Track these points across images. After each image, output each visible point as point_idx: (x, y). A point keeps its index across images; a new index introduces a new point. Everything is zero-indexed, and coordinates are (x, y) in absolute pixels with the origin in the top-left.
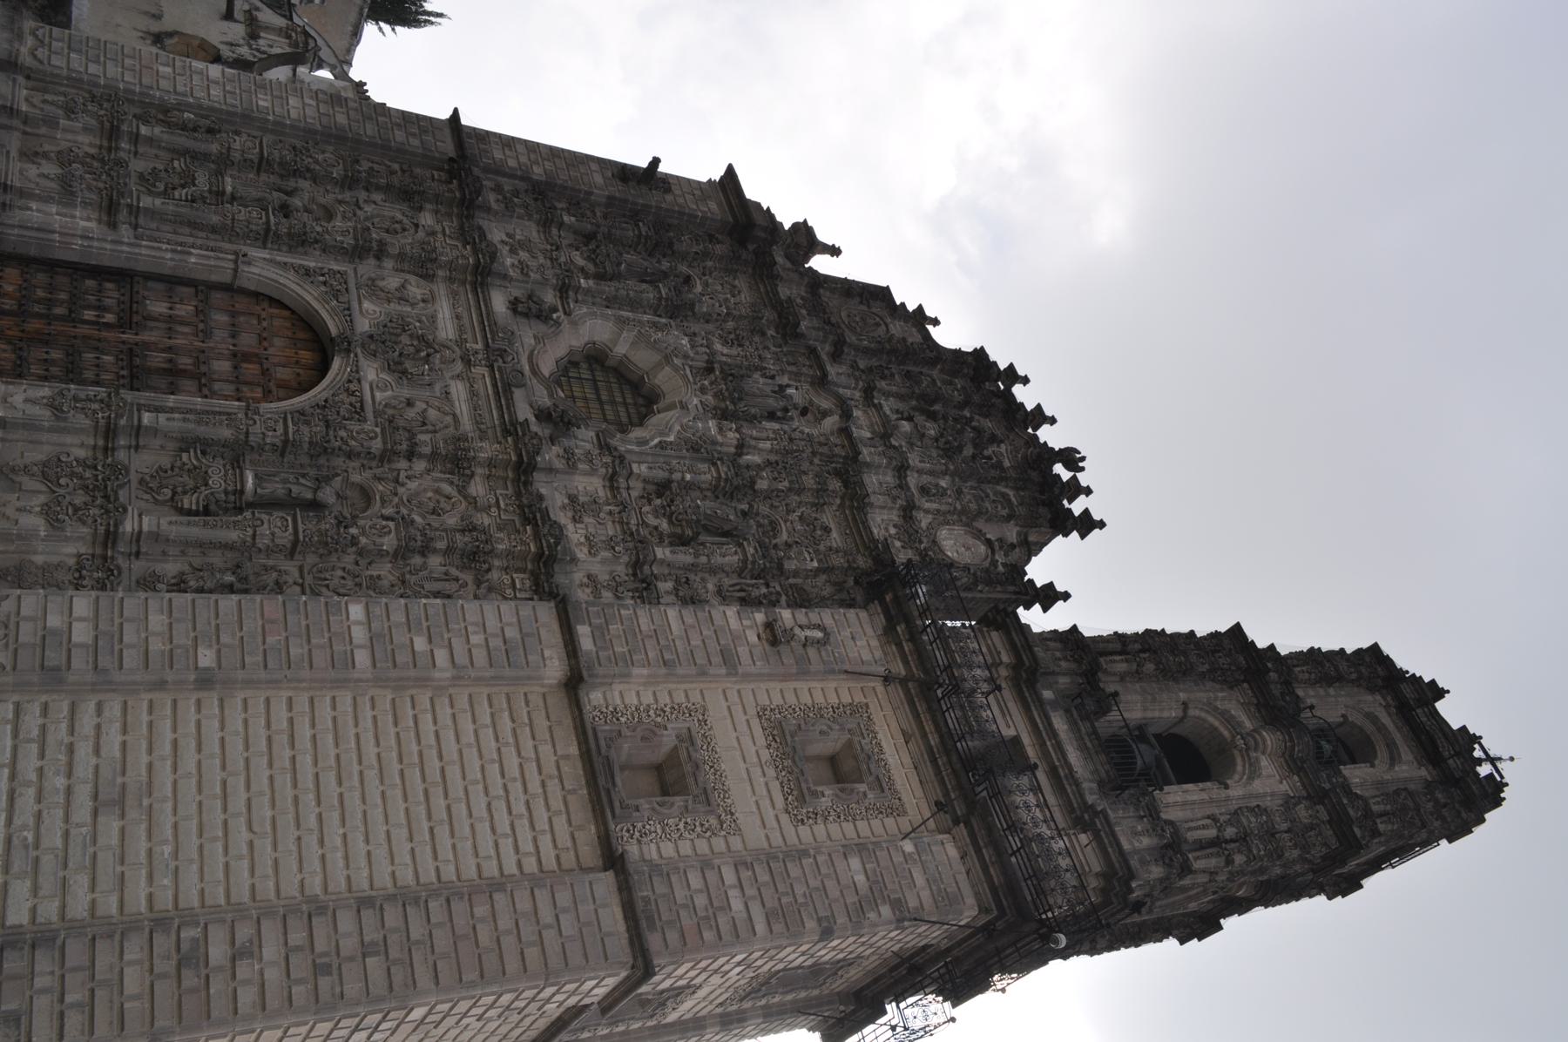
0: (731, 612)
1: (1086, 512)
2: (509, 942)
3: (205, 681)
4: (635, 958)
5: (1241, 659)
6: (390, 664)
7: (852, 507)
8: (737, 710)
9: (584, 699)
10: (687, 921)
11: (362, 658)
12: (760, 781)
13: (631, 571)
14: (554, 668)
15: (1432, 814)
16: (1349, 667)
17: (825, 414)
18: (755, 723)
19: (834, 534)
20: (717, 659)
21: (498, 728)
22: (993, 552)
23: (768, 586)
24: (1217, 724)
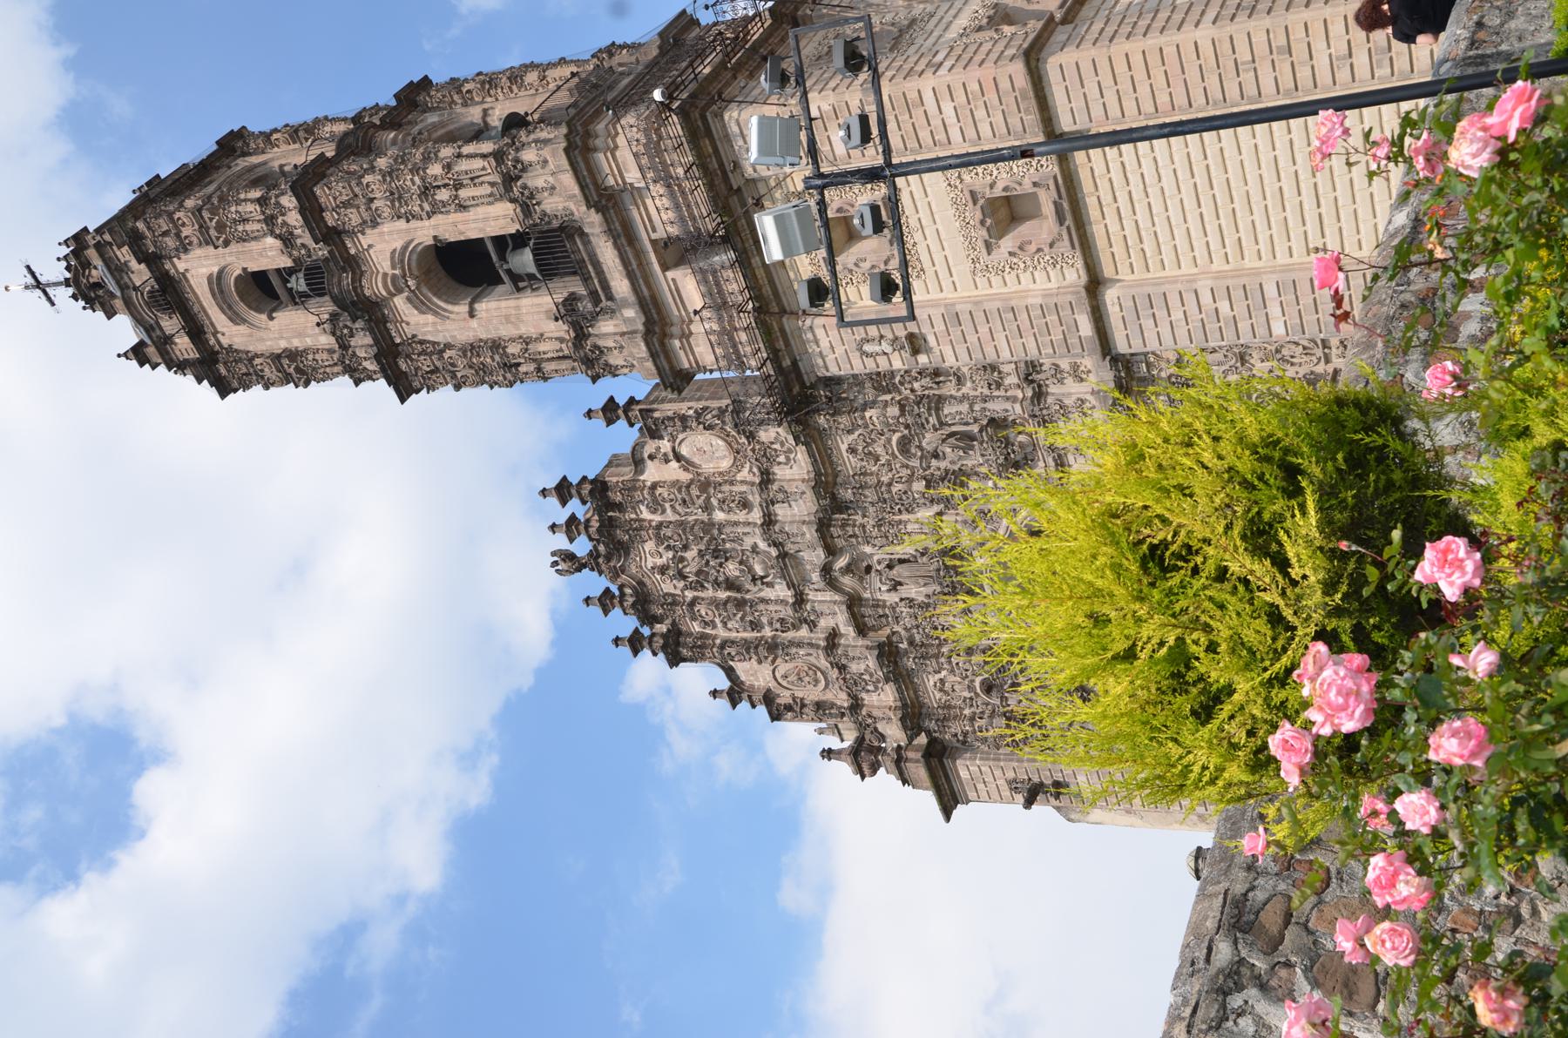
0: (950, 361)
1: (564, 503)
2: (1140, 75)
4: (1037, 67)
5: (403, 367)
6: (1248, 288)
7: (826, 475)
8: (943, 274)
9: (1083, 272)
10: (992, 96)
12: (924, 214)
13: (1044, 389)
14: (1110, 296)
15: (184, 224)
16: (262, 371)
17: (848, 570)
19: (844, 447)
20: (965, 318)
21: (1155, 243)
22: (674, 450)
23: (913, 390)
24: (435, 300)
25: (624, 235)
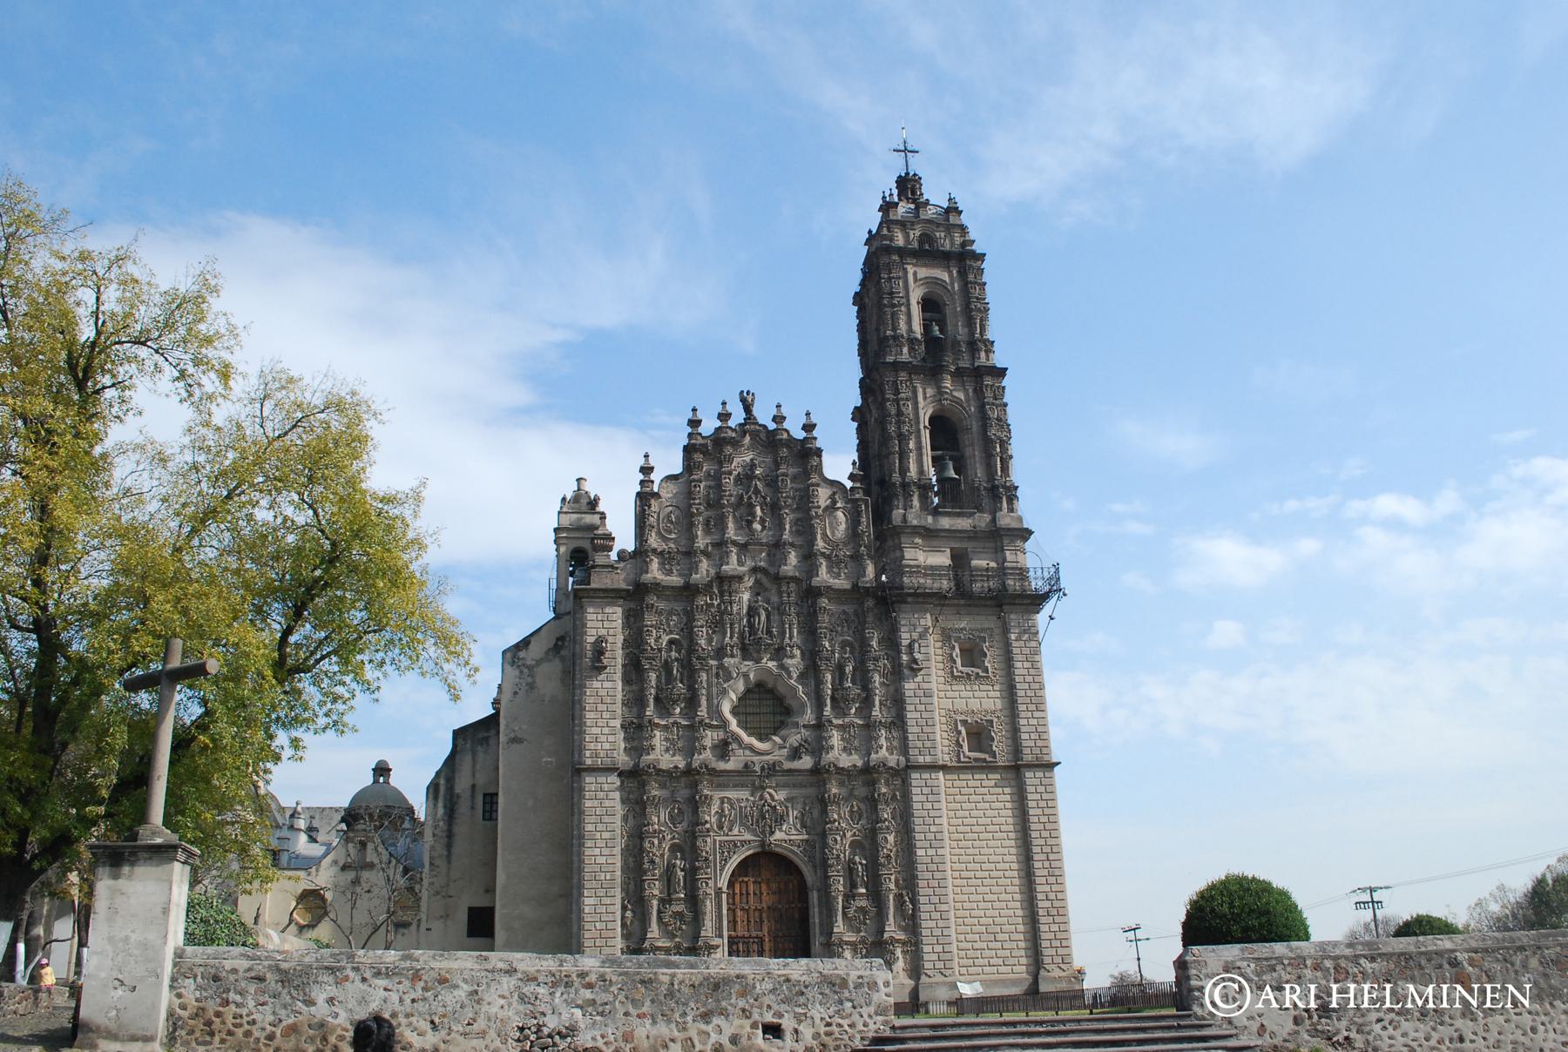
3: (950, 907)
10: (1039, 743)
11: (940, 852)
18: (954, 688)
25: (973, 535)
